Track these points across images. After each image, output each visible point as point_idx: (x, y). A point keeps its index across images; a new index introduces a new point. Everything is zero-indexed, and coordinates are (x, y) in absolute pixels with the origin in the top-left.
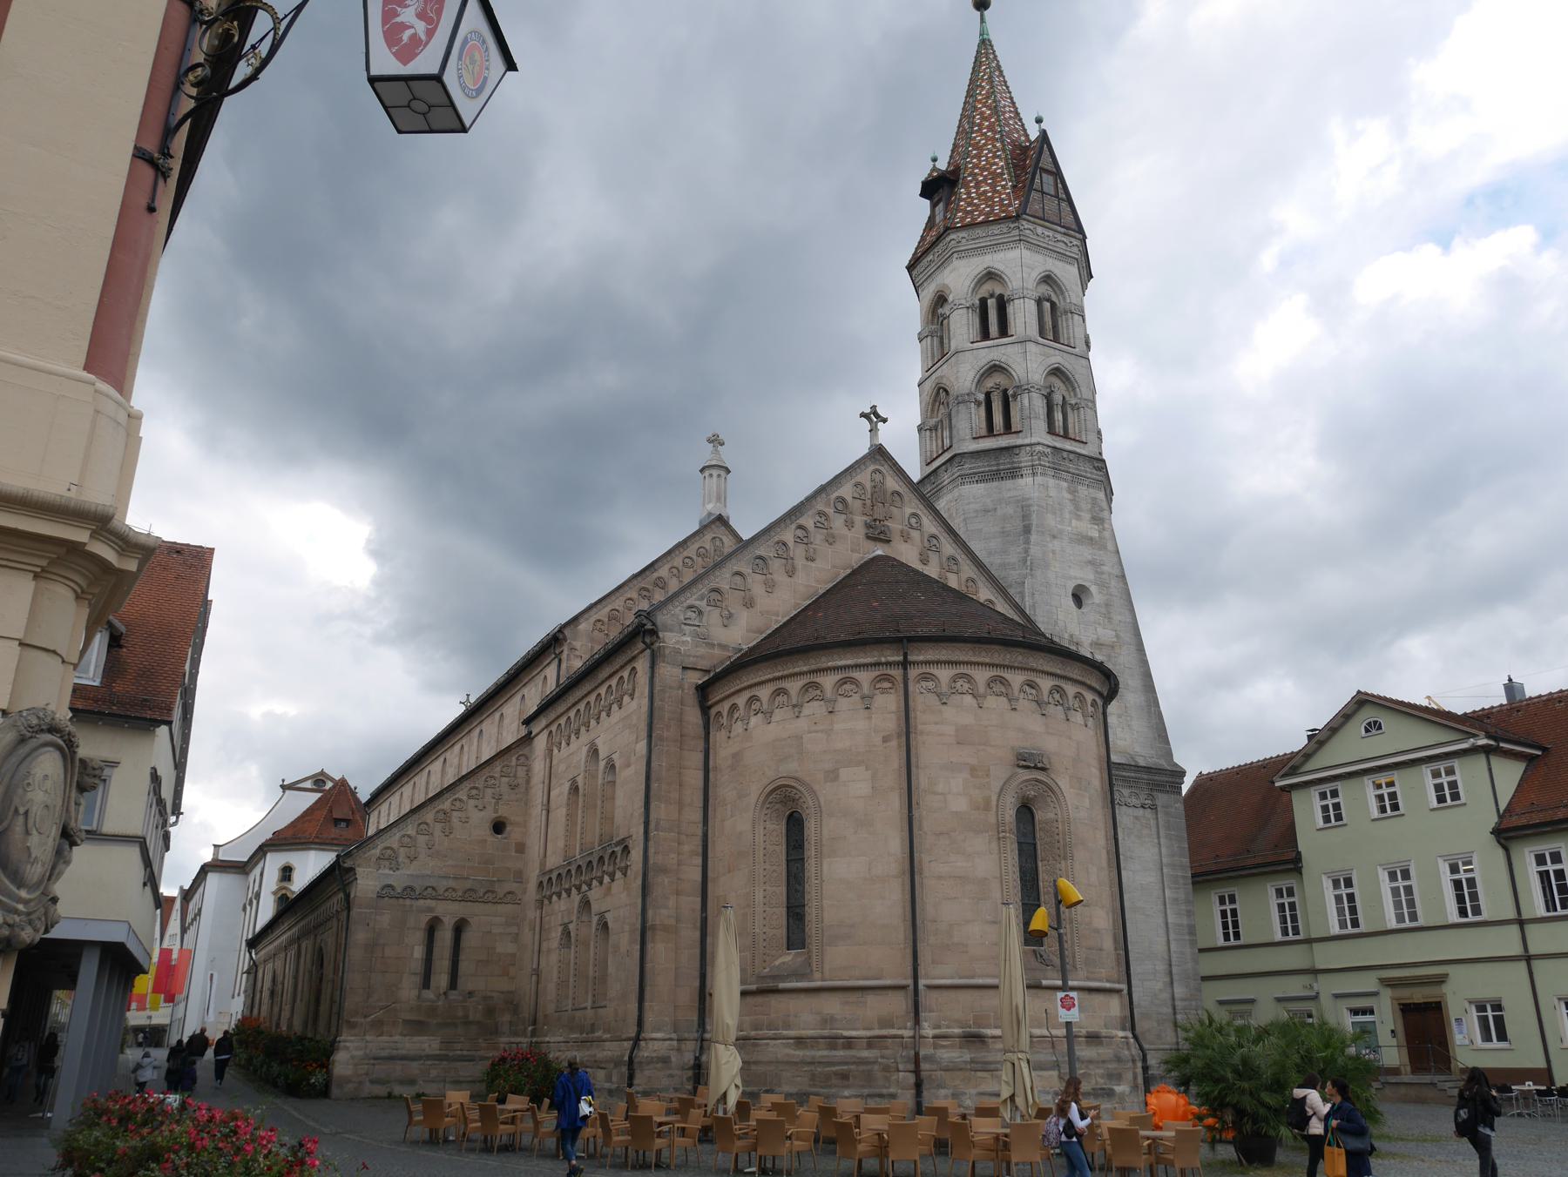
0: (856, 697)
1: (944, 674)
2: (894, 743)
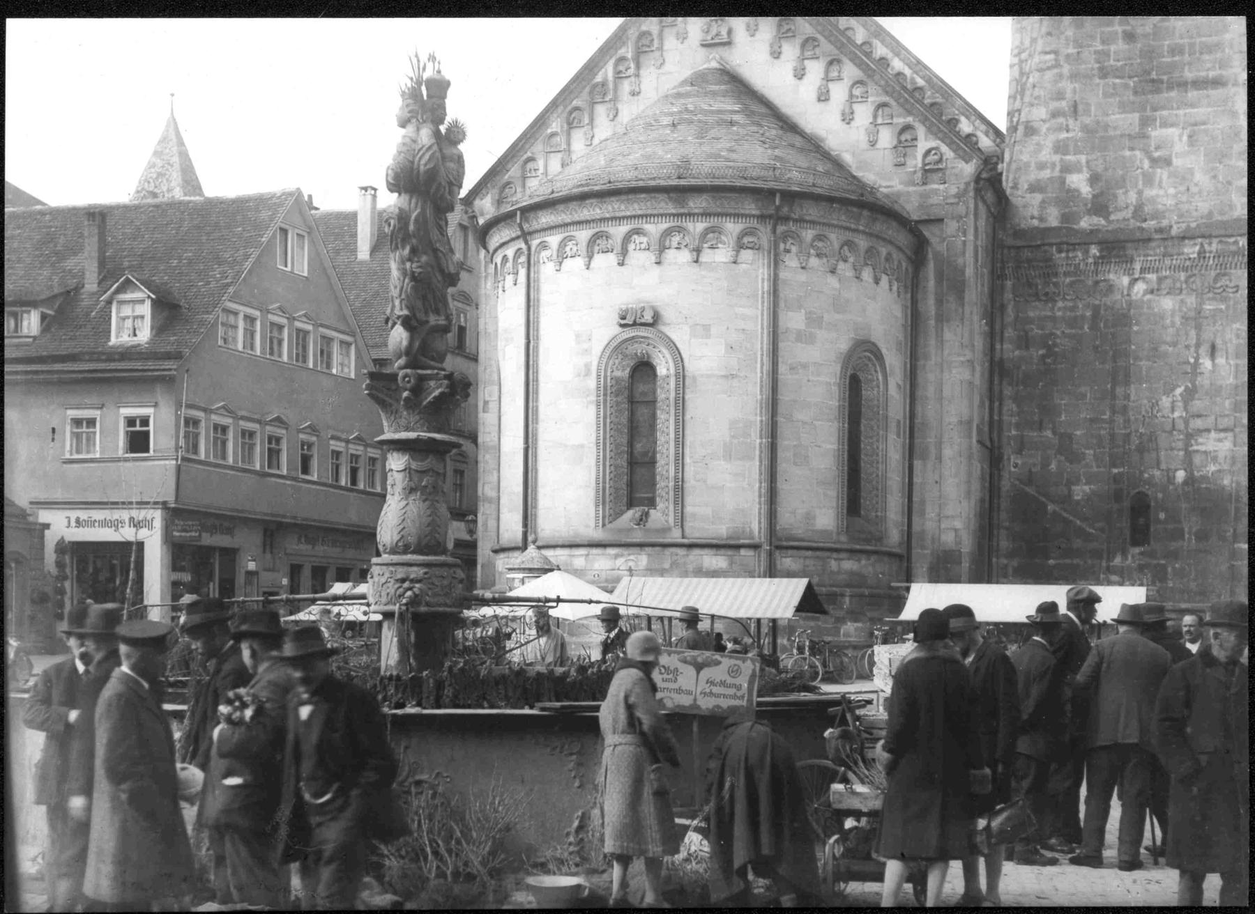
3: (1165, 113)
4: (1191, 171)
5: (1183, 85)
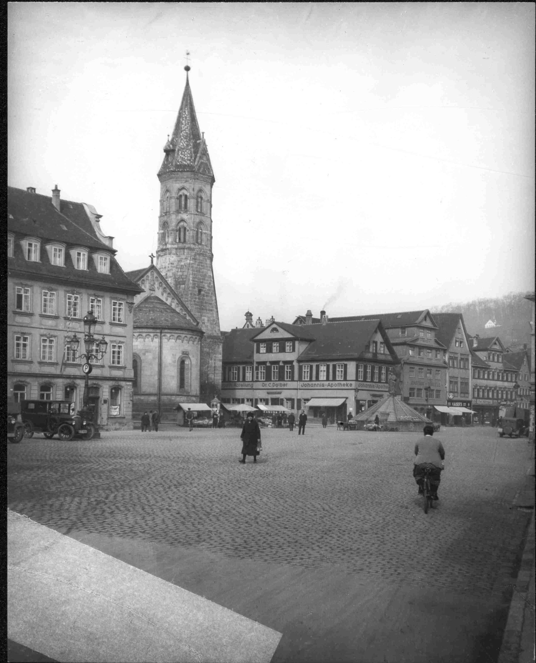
0: (150, 338)
1: (168, 335)
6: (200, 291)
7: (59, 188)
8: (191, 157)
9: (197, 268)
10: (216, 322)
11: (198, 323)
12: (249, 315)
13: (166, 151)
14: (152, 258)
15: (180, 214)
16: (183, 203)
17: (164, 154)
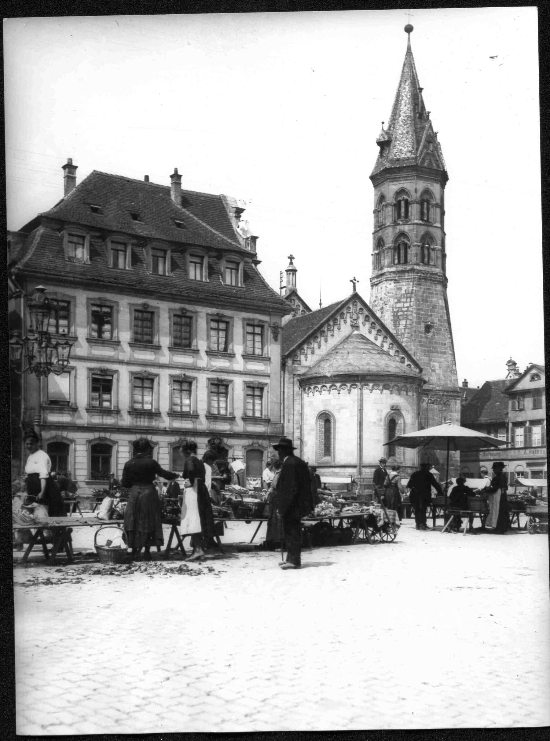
0: (346, 390)
1: (371, 385)
2: (356, 403)
3: (434, 358)
4: (440, 374)
5: (437, 352)
6: (428, 328)
7: (179, 173)
8: (413, 148)
9: (422, 296)
10: (452, 369)
11: (421, 370)
12: (512, 364)
13: (380, 143)
14: (354, 284)
15: (398, 227)
16: (403, 210)
17: (378, 148)
